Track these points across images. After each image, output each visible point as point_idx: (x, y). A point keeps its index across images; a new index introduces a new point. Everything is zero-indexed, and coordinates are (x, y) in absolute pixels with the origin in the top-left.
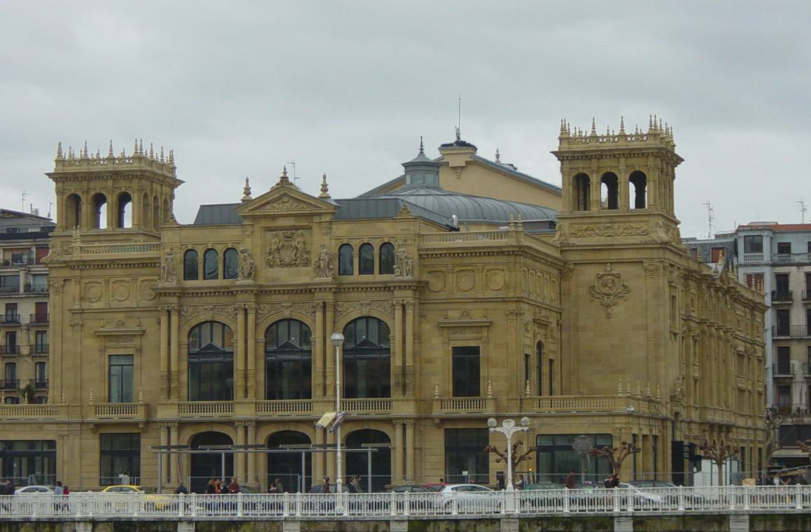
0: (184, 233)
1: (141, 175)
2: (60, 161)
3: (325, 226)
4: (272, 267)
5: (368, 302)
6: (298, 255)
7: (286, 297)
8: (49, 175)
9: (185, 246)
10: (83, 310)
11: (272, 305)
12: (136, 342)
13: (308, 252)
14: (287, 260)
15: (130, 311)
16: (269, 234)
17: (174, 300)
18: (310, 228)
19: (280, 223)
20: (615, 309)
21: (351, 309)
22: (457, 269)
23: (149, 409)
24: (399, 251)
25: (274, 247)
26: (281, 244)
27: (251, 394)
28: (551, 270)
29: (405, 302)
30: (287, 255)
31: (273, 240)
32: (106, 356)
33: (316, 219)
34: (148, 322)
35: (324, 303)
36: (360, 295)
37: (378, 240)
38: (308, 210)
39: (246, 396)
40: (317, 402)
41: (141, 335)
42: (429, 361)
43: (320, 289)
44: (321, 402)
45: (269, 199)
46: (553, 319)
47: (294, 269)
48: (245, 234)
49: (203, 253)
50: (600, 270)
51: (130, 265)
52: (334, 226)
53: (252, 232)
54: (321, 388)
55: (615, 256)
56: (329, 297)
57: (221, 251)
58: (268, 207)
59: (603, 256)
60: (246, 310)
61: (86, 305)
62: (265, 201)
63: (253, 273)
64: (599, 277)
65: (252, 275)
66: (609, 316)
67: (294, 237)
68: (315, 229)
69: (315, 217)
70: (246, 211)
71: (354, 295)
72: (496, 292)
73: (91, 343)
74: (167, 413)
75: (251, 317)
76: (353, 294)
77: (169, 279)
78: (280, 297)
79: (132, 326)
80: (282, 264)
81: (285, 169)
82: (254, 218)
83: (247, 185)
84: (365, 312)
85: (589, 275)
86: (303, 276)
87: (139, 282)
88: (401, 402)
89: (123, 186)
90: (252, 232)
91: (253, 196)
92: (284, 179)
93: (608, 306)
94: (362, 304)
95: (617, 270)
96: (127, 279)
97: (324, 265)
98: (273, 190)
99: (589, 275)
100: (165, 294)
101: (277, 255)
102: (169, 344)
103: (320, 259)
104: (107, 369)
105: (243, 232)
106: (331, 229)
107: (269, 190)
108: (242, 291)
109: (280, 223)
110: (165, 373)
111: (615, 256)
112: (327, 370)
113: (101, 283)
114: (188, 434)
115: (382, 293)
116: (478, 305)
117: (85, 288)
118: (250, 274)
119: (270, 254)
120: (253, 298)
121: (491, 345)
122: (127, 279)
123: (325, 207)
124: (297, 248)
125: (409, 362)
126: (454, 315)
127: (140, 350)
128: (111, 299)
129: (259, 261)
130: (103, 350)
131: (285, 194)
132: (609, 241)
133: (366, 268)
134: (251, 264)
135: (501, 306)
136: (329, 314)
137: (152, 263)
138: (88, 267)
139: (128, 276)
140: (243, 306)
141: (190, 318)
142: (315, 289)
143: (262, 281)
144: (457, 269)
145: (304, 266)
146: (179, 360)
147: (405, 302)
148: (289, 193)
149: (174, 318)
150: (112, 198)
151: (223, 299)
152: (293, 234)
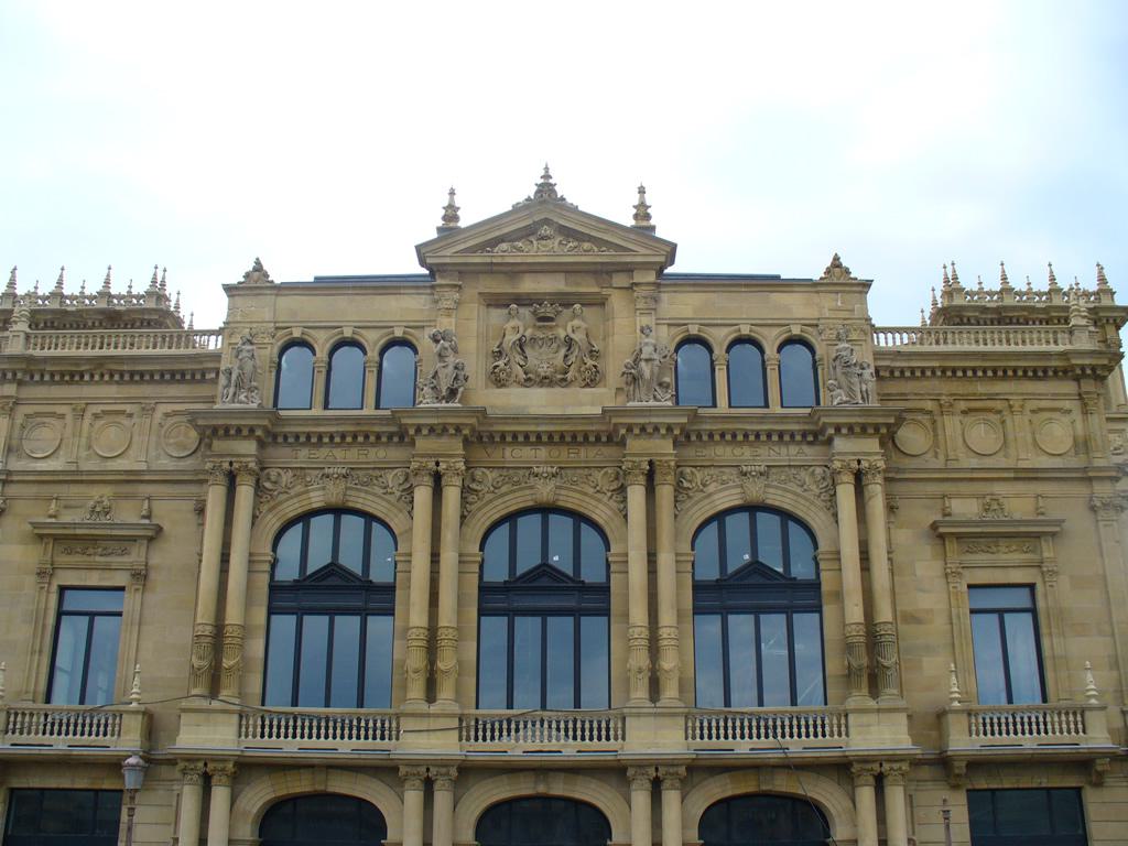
0: (285, 303)
3: (644, 294)
4: (503, 386)
5: (762, 469)
6: (572, 358)
7: (543, 453)
9: (280, 333)
10: (9, 473)
11: (505, 472)
12: (136, 556)
13: (593, 354)
14: (544, 370)
15: (132, 479)
17: (248, 447)
18: (600, 302)
19: (528, 285)
21: (712, 488)
22: (963, 405)
25: (511, 338)
26: (529, 333)
27: (446, 692)
29: (865, 464)
30: (543, 360)
32: (54, 588)
33: (620, 280)
34: (171, 511)
35: (651, 463)
36: (738, 451)
37: (776, 331)
38: (606, 257)
39: (431, 696)
40: (638, 715)
41: (151, 539)
42: (912, 619)
43: (643, 429)
44: (650, 715)
45: (506, 230)
47: (557, 390)
48: (440, 305)
49: (328, 346)
51: (142, 374)
52: (665, 297)
53: (458, 303)
56: (664, 448)
57: (375, 344)
58: (504, 246)
62: (495, 233)
63: (461, 390)
65: (459, 396)
67: (560, 320)
68: (617, 301)
69: (614, 275)
70: (449, 252)
71: (724, 453)
72: (1058, 459)
74: (210, 734)
75: (452, 495)
76: (720, 450)
77: (242, 397)
78: (526, 453)
79: (128, 514)
80: (529, 379)
81: (547, 169)
83: (452, 199)
84: (755, 491)
86: (585, 403)
87: (158, 415)
88: (873, 718)
90: (458, 303)
91: (462, 224)
92: (546, 189)
94: (745, 475)
96: (128, 408)
97: (652, 373)
98: (517, 209)
100: (227, 429)
101: (519, 358)
102: (225, 559)
103: (637, 361)
104: (51, 620)
105: (436, 302)
106: (656, 300)
107: (511, 208)
108: (432, 430)
110: (208, 630)
112: (664, 632)
113: (62, 416)
114: (258, 796)
115: (793, 449)
116: (1021, 487)
117: (23, 427)
118: (453, 393)
119: (499, 354)
120: (457, 447)
121: (1064, 583)
122: (128, 408)
123: (643, 251)
124: (569, 343)
125: (884, 613)
126: (965, 508)
127: (141, 576)
128: (84, 454)
129: (476, 367)
131: (547, 221)
134: (456, 368)
135: (1081, 490)
136: (665, 493)
138: (37, 378)
140: (432, 465)
142: (630, 429)
144: (963, 405)
145: (587, 385)
146: (249, 602)
147: (865, 464)
148: (555, 220)
149: (245, 493)
151: (378, 454)
152: (558, 313)
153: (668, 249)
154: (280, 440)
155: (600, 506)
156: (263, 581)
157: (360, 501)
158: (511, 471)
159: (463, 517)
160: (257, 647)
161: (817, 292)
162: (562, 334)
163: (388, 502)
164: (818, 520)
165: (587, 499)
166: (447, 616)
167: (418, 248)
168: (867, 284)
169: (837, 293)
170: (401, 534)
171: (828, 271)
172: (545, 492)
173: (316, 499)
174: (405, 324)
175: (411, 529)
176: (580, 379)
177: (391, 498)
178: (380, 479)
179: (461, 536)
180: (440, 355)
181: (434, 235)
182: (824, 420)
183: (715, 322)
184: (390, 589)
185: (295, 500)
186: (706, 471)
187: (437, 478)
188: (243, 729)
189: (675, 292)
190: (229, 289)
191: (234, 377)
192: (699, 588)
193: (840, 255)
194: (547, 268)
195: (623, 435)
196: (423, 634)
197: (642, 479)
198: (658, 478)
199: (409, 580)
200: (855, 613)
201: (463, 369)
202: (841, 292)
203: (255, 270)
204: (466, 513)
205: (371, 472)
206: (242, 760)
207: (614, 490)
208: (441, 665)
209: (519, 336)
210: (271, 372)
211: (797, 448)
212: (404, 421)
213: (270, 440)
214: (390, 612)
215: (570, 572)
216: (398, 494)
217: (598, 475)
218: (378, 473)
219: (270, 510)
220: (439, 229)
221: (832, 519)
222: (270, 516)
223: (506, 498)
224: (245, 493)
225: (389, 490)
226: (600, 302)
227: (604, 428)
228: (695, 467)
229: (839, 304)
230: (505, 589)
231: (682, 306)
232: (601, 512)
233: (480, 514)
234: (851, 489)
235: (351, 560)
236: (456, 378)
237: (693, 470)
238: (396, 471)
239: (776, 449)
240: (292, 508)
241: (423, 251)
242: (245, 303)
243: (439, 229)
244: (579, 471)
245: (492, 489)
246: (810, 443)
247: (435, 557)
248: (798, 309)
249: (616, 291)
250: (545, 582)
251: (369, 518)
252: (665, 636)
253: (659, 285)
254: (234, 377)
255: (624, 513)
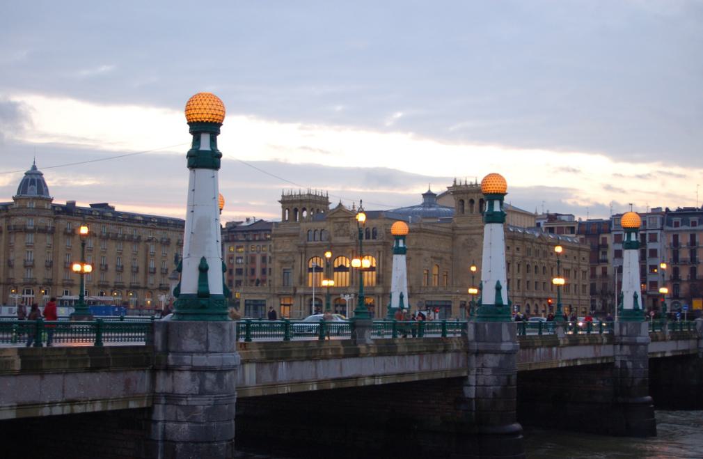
1: (309, 201)
2: (283, 196)
8: (279, 201)
16: (336, 224)
18: (349, 222)
20: (472, 253)
23: (295, 289)
24: (378, 231)
28: (446, 237)
30: (342, 232)
31: (337, 226)
46: (447, 257)
50: (466, 237)
55: (473, 231)
59: (468, 232)
61: (276, 250)
64: (466, 240)
66: (470, 255)
73: (278, 265)
79: (291, 258)
82: (331, 218)
85: (463, 238)
86: (346, 240)
89: (304, 205)
93: (469, 251)
95: (473, 237)
99: (463, 238)
111: (473, 231)
125: (381, 273)
127: (293, 267)
130: (281, 267)
132: (470, 225)
133: (368, 238)
137: (296, 235)
143: (332, 242)
150: (300, 210)
224: (303, 256)
226: (349, 222)
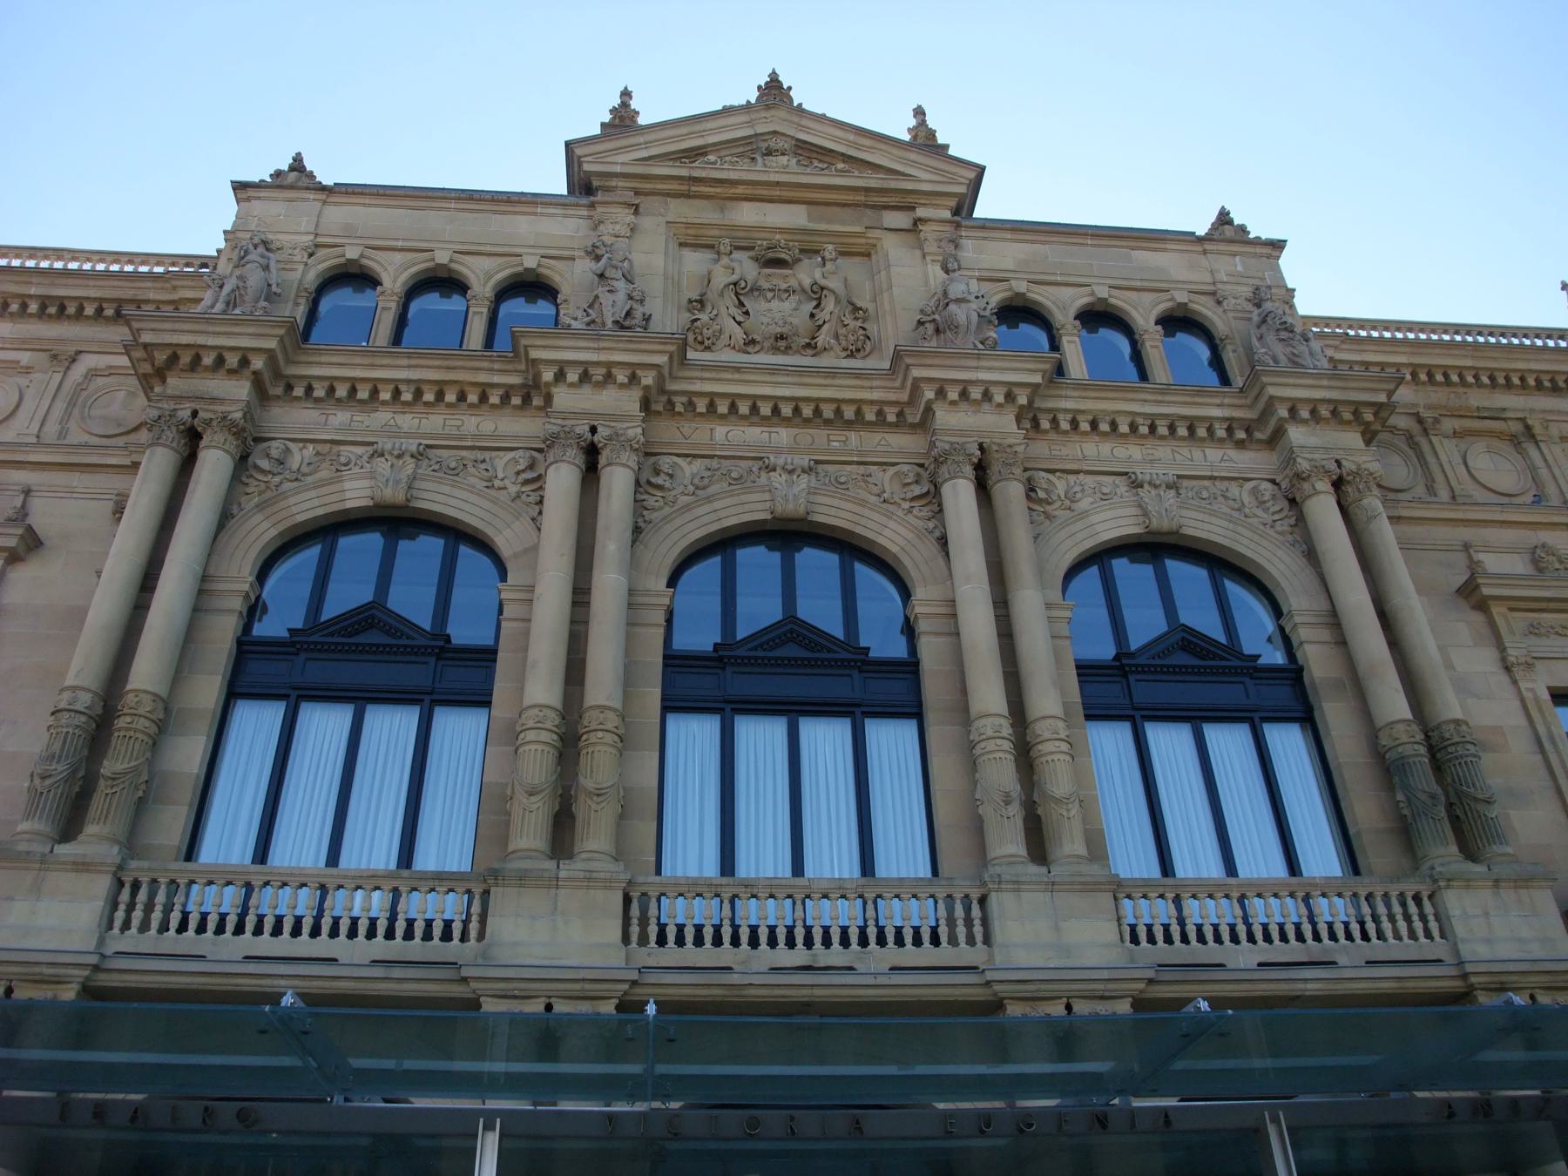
0: (337, 215)
4: (708, 348)
7: (783, 435)
11: (714, 463)
19: (747, 215)
21: (1084, 504)
22: (1457, 424)
35: (981, 447)
54: (1018, 823)
56: (1000, 425)
60: (592, 454)
68: (893, 249)
71: (1095, 450)
75: (617, 482)
78: (753, 435)
80: (753, 342)
87: (78, 371)
92: (774, 91)
96: (25, 358)
109: (747, 215)
115: (1214, 454)
122: (25, 358)
136: (1010, 493)
139: (22, 344)
140: (583, 429)
141: (287, 486)
145: (852, 355)
151: (475, 424)
153: (972, 175)
154: (299, 391)
155: (891, 524)
156: (223, 631)
157: (440, 498)
158: (728, 462)
159: (637, 531)
160: (188, 754)
161: (1205, 252)
162: (807, 282)
163: (494, 501)
164: (1275, 559)
165: (867, 512)
166: (602, 685)
167: (569, 145)
168: (1278, 246)
169: (1234, 255)
170: (516, 556)
171: (1214, 227)
172: (789, 496)
173: (356, 493)
174: (542, 251)
175: (535, 548)
176: (837, 349)
177: (502, 495)
178: (483, 466)
179: (633, 564)
180: (601, 276)
181: (598, 131)
182: (1272, 391)
183: (1053, 278)
184: (486, 656)
185: (313, 493)
186: (1072, 478)
187: (592, 454)
188: (120, 915)
189: (985, 238)
190: (241, 188)
191: (227, 289)
192: (1086, 670)
193: (1228, 208)
194: (783, 198)
195: (929, 402)
196: (552, 720)
197: (969, 470)
198: (995, 470)
199: (526, 634)
200: (1393, 704)
201: (642, 302)
202: (1241, 254)
203: (292, 169)
204: (641, 524)
205: (464, 453)
206: (104, 980)
207: (913, 499)
208: (586, 782)
209: (735, 278)
210: (297, 304)
211: (1220, 453)
212: (534, 354)
213: (279, 391)
214: (481, 700)
215: (839, 632)
216: (513, 489)
217: (885, 478)
218: (480, 455)
219: (260, 507)
220: (603, 125)
221: (1302, 562)
222: (259, 517)
223: (717, 505)
225: (497, 483)
227: (892, 396)
228: (1052, 471)
229: (1239, 268)
230: (722, 658)
231: (1005, 256)
232: (893, 532)
233: (668, 528)
234: (1331, 501)
235: (412, 600)
236: (628, 314)
237: (1050, 476)
238: (511, 455)
239: (1185, 452)
240: (307, 506)
241: (578, 152)
242: (271, 210)
243: (603, 125)
244: (849, 468)
245: (691, 488)
246: (1240, 444)
247: (581, 596)
248: (1183, 277)
249: (890, 235)
250: (791, 651)
251: (456, 534)
252: (1047, 735)
253: (958, 226)
254: (227, 289)
255: (937, 534)
